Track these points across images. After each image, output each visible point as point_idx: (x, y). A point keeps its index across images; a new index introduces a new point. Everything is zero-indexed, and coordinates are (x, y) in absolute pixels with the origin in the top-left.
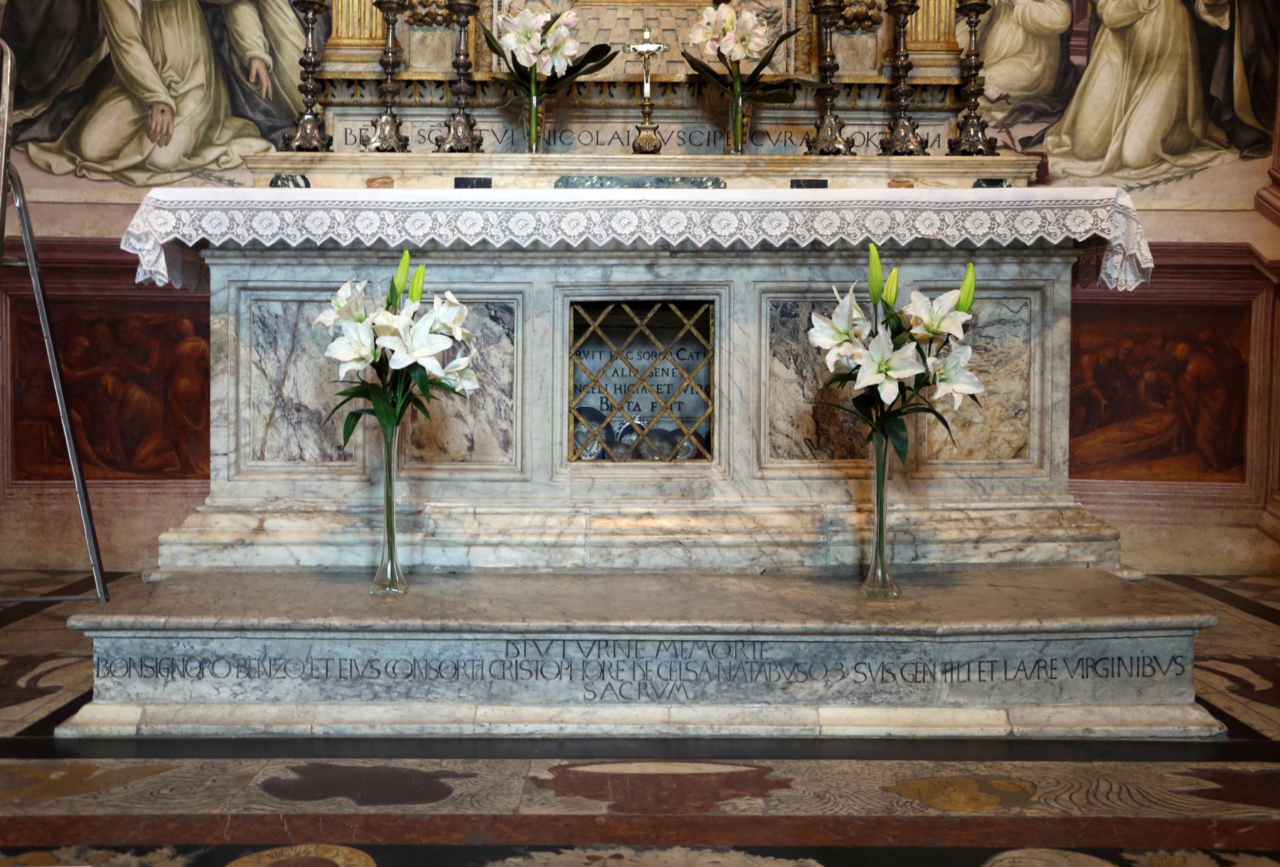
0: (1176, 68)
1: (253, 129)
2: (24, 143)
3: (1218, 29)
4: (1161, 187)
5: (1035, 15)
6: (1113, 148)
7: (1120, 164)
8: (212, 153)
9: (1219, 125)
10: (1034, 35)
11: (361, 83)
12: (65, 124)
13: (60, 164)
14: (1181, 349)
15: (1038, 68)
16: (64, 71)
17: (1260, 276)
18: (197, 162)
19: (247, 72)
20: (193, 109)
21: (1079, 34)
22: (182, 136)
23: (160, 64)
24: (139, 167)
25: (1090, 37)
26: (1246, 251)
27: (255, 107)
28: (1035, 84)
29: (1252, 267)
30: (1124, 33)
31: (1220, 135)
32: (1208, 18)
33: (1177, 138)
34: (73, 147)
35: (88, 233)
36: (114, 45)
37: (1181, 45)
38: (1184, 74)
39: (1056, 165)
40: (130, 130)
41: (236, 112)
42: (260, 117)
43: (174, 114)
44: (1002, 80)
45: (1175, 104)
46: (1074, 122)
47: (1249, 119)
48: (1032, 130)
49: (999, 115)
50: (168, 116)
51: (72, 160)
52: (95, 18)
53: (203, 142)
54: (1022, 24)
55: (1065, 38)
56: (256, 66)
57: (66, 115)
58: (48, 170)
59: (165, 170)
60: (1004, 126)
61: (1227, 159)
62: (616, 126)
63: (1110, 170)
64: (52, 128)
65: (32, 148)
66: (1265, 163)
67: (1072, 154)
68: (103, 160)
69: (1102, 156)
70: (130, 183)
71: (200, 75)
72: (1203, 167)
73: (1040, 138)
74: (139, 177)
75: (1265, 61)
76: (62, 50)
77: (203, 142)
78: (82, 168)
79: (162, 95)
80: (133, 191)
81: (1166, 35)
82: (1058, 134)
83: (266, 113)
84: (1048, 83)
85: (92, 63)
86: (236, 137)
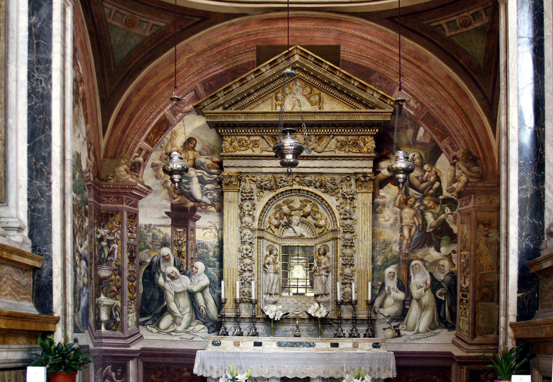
0: (431, 309)
1: (201, 323)
2: (146, 325)
3: (442, 300)
4: (429, 338)
5: (397, 296)
6: (417, 328)
7: (418, 332)
8: (191, 328)
9: (443, 323)
10: (396, 301)
11: (231, 318)
12: (156, 321)
13: (155, 330)
14: (434, 377)
15: (397, 309)
16: (156, 308)
17: (454, 360)
18: (187, 330)
19: (199, 309)
20: (186, 318)
21: (407, 301)
22: (184, 324)
23: (178, 307)
24: (173, 331)
25: (410, 301)
26: (450, 353)
27: (201, 317)
28: (397, 312)
29: (452, 357)
30: (419, 300)
31: (443, 325)
32: (439, 297)
33: (433, 326)
34: (158, 326)
35: (161, 347)
36: (167, 302)
37: (433, 304)
38: (434, 311)
39: (402, 332)
40: (171, 322)
41: (197, 318)
42: (203, 320)
43: (182, 319)
44: (388, 312)
45: (432, 318)
46: (407, 322)
47: (450, 321)
48: (396, 324)
49: (388, 320)
50: (180, 319)
51: (157, 329)
52: (163, 296)
53: (189, 326)
54: (393, 298)
55: (404, 301)
56: (202, 307)
57: (156, 319)
58: (152, 332)
59: (180, 332)
60: (389, 323)
61: (445, 331)
62: (291, 327)
63: (416, 334)
64: (153, 322)
65: (148, 327)
66: (454, 332)
67: (406, 330)
68: (165, 330)
69: (414, 330)
70: (171, 335)
71: (188, 310)
72: (439, 333)
73: (398, 326)
74: (173, 334)
75: (453, 308)
76: (155, 303)
77: (189, 326)
78: (159, 332)
79: (179, 314)
80: (172, 337)
81: (429, 301)
82: (403, 325)
83: (204, 319)
84: (400, 312)
85: (162, 306)
86: (197, 324)
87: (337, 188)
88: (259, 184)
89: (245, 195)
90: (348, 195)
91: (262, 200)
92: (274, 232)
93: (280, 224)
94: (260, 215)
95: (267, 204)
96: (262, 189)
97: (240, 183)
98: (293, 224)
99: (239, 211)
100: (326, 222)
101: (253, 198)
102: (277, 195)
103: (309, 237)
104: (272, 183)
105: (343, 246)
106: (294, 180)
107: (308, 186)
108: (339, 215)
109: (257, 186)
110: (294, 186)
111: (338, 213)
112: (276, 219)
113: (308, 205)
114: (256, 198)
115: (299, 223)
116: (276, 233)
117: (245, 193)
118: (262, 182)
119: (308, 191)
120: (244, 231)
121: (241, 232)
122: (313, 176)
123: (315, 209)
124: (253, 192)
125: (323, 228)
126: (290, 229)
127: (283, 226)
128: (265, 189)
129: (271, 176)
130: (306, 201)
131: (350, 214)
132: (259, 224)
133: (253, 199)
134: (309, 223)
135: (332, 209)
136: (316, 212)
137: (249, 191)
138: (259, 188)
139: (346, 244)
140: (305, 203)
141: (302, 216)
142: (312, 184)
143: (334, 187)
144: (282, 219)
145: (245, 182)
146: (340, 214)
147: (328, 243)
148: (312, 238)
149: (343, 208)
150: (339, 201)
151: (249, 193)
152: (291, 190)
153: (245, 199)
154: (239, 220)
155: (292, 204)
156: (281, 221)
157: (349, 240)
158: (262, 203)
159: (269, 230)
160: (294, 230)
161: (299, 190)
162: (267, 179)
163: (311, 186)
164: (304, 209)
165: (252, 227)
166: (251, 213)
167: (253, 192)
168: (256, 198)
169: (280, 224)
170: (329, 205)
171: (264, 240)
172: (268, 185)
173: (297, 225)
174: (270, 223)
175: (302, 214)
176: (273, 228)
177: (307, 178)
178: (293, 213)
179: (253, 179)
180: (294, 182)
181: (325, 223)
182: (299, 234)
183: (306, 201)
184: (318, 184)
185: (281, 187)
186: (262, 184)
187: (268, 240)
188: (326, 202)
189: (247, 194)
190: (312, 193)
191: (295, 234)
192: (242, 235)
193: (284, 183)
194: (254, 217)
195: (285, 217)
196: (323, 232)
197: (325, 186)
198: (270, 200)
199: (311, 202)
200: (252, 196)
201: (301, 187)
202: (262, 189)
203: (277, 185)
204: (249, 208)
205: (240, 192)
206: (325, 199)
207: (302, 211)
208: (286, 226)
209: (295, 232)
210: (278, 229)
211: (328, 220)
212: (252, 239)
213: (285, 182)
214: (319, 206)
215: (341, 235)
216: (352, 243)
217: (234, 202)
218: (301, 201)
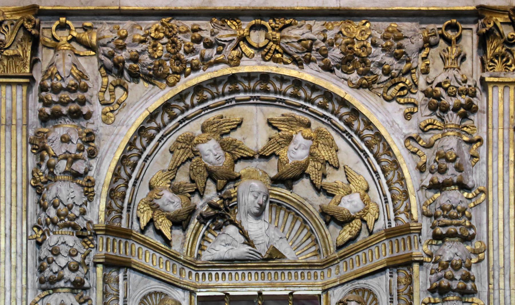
87: (409, 72)
88: (111, 56)
89: (55, 98)
90: (452, 95)
91: (121, 116)
92: (168, 242)
93: (192, 211)
94: (116, 175)
95: (141, 131)
96: (120, 74)
97: (35, 51)
98: (242, 209)
99: (32, 161)
100: (366, 201)
101: (85, 110)
102: (181, 97)
103: (301, 259)
104: (161, 50)
105: (432, 291)
106: (244, 39)
107: (296, 62)
108: (415, 173)
109: (102, 66)
110: (244, 61)
111: (413, 166)
112: (176, 190)
113: (299, 138)
114: (98, 109)
115: (262, 208)
116: (176, 247)
117: (56, 90)
118: (123, 48)
119: (298, 83)
120: (52, 240)
121: (39, 244)
122: (317, 25)
123: (324, 153)
124: (85, 89)
125: (356, 224)
126: (231, 229)
127: (203, 219)
128: (135, 76)
129: (153, 24)
130: (290, 121)
131: (459, 169)
132: (109, 209)
133: (88, 116)
134: (301, 206)
135: (388, 150)
136: (326, 162)
137: (71, 81)
138: (109, 71)
139: (445, 283)
140: (285, 131)
141: (276, 181)
142: (314, 55)
143: (396, 66)
144: (200, 193)
145: (56, 48)
146: (421, 169)
147: (372, 283)
148: (311, 266)
149: (429, 146)
150: (414, 121)
151: (68, 89)
152: (232, 79)
153: (56, 116)
154: (33, 197)
155: (235, 136)
156: (196, 199)
157: (456, 268)
158: (124, 130)
159: (150, 236)
160: (243, 233)
161: (265, 77)
162: (139, 35)
163: (309, 61)
164: (283, 153)
165: (81, 223)
166: (79, 167)
167: (85, 89)
168: (98, 109)
169: (192, 211)
170: (378, 134)
171: (132, 276)
172: (145, 59)
173: (258, 216)
174: (154, 207)
175: (273, 174)
176: (165, 226)
177: (295, 33)
178: (240, 168)
179: (85, 37)
180: (244, 47)
181: (361, 206)
182: (263, 250)
183: (290, 121)
184: (336, 53)
185: (195, 69)
186: (123, 55)
187: (147, 274)
188: (369, 124)
189: (64, 95)
190: (314, 88)
191: (246, 248)
192: (44, 252)
193: (208, 53)
194: (91, 183)
195: (211, 188)
196: (352, 240)
197: (363, 61)
198: (152, 117)
199: (308, 125)
200: (83, 102)
201: (271, 68)
202: (120, 74)
203: (178, 59)
204: (73, 149)
205: (36, 88)
206: (364, 110)
207: (274, 161)
208: (214, 218)
209: (249, 242)
210: (185, 229)
211: (374, 193)
212: (82, 271)
213: (209, 45)
214: (340, 142)
215: (427, 249)
216: (467, 278)
217: (9, 125)
218: (269, 124)
